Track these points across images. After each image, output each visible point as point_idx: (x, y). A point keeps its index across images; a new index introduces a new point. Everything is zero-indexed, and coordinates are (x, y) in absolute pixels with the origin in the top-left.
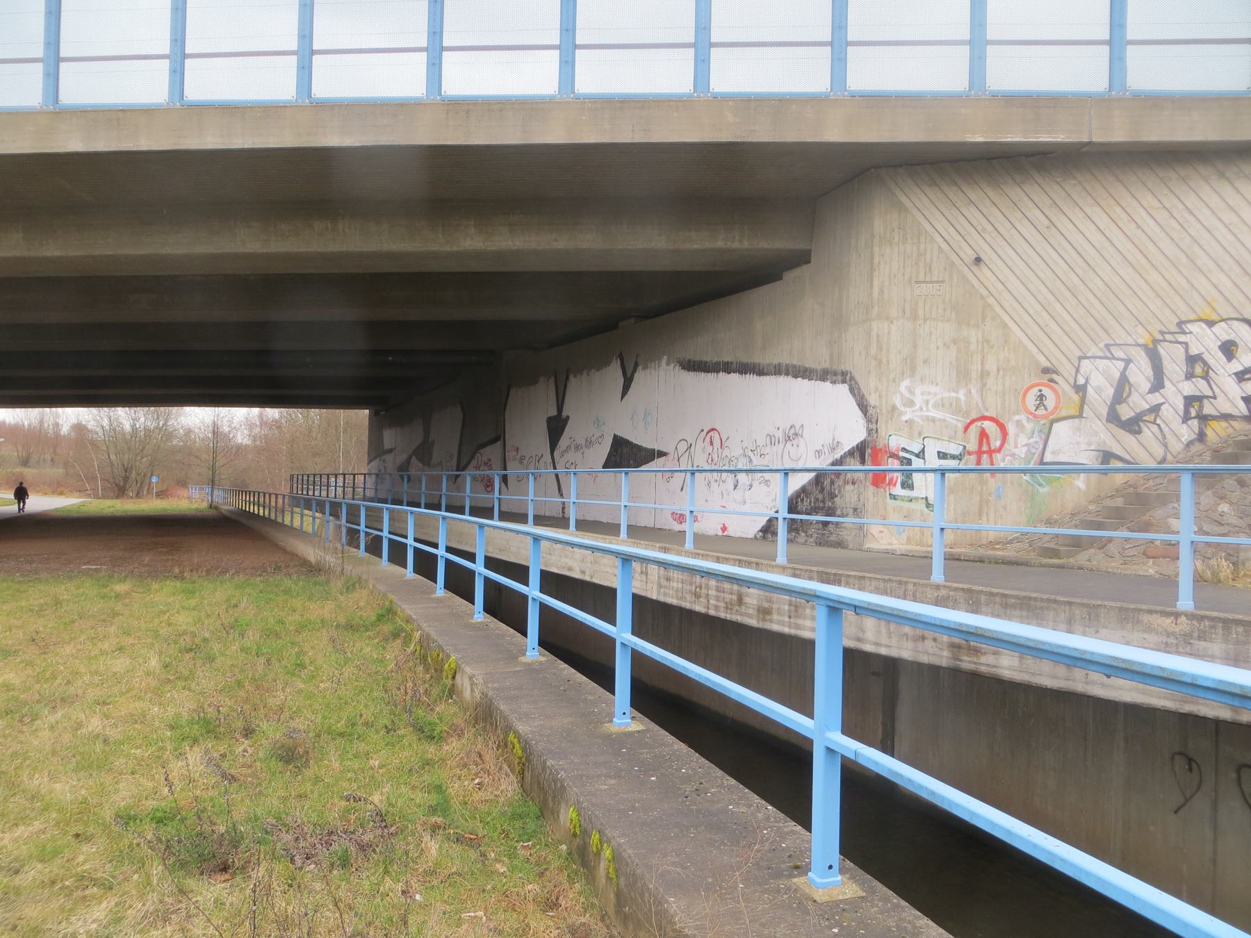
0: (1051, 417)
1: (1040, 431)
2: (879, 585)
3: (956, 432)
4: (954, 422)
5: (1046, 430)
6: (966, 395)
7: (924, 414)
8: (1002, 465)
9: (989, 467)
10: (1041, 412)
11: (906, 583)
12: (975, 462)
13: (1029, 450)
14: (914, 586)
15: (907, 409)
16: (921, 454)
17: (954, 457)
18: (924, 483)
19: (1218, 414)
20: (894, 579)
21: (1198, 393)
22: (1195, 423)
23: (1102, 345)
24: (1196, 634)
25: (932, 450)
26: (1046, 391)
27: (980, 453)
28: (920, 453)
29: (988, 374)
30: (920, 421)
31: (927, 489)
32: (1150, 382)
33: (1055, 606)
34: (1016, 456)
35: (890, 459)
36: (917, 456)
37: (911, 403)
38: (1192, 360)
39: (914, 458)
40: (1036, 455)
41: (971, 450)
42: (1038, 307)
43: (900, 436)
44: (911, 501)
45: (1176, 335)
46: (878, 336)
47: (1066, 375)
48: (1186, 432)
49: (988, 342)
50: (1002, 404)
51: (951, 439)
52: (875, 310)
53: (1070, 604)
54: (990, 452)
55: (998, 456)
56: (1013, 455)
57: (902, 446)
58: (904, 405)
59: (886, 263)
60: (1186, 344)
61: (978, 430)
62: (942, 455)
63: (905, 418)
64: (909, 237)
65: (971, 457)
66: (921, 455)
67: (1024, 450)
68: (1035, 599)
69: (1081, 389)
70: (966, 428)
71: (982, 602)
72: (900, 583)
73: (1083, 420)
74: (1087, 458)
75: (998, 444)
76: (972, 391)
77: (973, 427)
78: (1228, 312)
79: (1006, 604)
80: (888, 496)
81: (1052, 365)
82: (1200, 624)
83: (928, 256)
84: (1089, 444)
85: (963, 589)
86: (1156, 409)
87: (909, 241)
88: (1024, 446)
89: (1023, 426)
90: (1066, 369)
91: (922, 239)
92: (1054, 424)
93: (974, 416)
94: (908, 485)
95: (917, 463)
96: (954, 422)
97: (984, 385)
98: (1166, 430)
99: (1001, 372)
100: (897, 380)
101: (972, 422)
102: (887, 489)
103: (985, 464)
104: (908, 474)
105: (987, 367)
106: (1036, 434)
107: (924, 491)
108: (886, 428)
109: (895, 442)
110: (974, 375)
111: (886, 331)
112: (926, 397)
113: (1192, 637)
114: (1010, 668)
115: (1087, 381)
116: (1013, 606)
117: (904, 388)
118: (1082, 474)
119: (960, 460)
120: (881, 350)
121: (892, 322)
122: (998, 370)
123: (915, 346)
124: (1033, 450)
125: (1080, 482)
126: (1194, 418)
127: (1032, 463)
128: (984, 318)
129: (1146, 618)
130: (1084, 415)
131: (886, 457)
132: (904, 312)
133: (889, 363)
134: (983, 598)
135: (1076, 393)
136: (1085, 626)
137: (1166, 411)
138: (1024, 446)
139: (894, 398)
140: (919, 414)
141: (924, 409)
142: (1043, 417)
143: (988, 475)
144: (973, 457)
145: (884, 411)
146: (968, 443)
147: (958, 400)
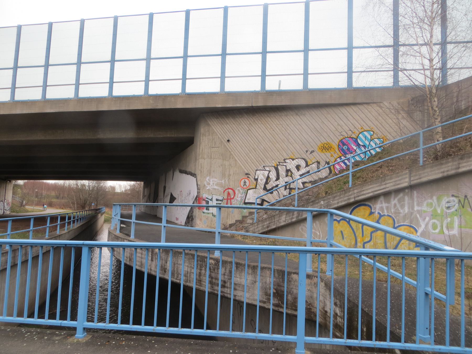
4: (221, 190)
5: (246, 192)
7: (213, 187)
10: (245, 187)
13: (241, 199)
15: (208, 186)
17: (220, 200)
23: (262, 166)
26: (247, 181)
27: (228, 199)
29: (231, 175)
31: (213, 210)
37: (209, 184)
38: (288, 171)
39: (209, 201)
49: (231, 165)
52: (201, 156)
54: (231, 199)
55: (233, 200)
56: (237, 200)
60: (286, 166)
61: (227, 192)
62: (217, 200)
63: (207, 188)
64: (210, 134)
66: (211, 200)
69: (256, 180)
70: (224, 192)
73: (257, 189)
75: (233, 196)
77: (226, 191)
83: (215, 140)
87: (210, 135)
89: (240, 191)
90: (252, 173)
91: (214, 135)
93: (226, 188)
96: (221, 190)
97: (229, 178)
98: (280, 193)
99: (234, 175)
106: (243, 194)
107: (212, 211)
111: (203, 162)
112: (213, 182)
119: (222, 201)
120: (202, 168)
122: (233, 174)
123: (211, 167)
124: (242, 199)
126: (288, 189)
128: (230, 158)
140: (211, 187)
142: (245, 188)
147: (222, 183)
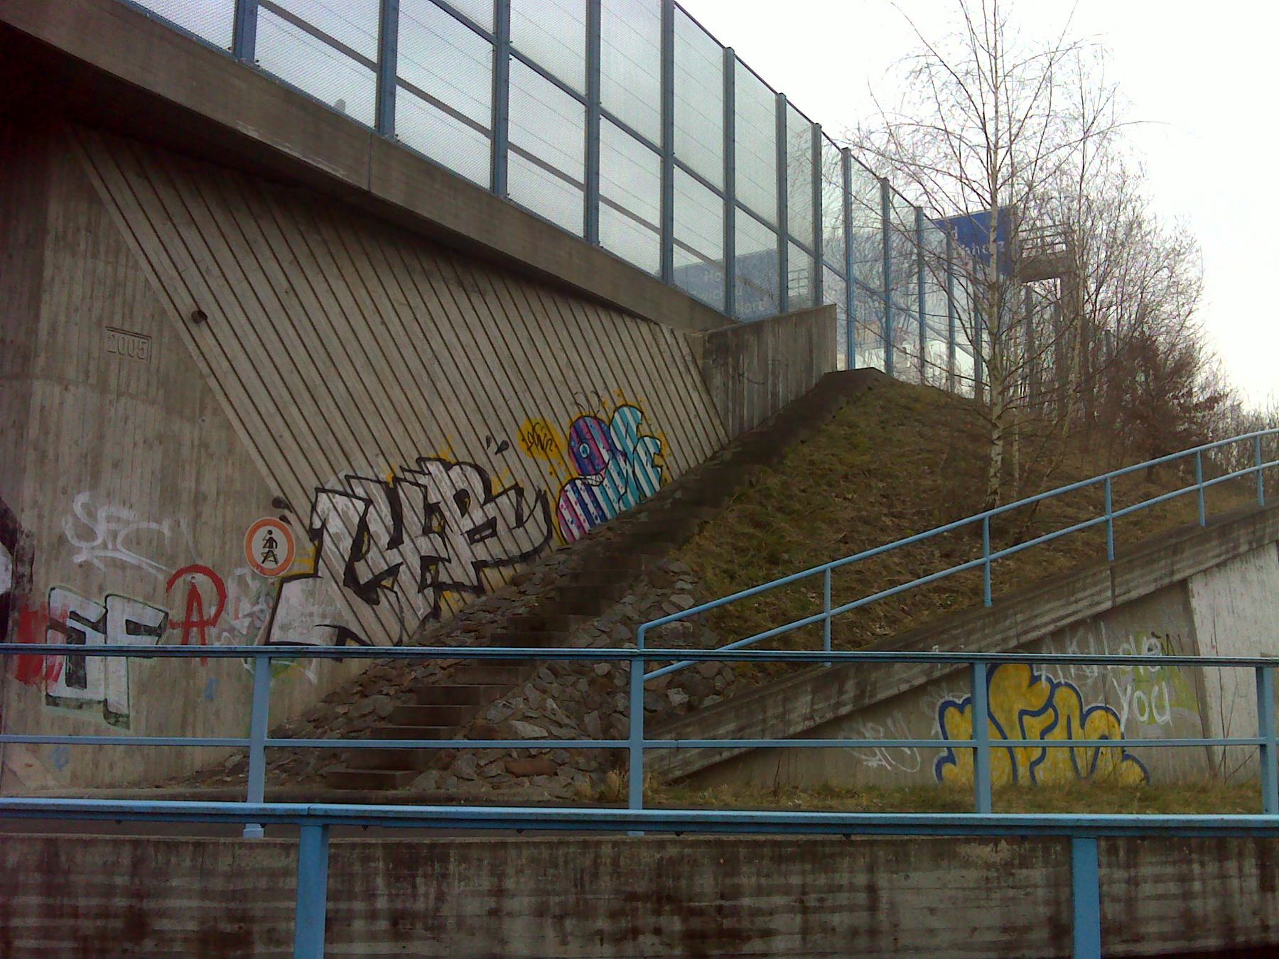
0: (281, 574)
1: (268, 594)
2: (541, 854)
3: (154, 590)
4: (153, 571)
5: (274, 594)
6: (172, 529)
7: (110, 554)
8: (217, 645)
9: (198, 646)
10: (269, 565)
11: (598, 844)
12: (180, 640)
13: (252, 624)
14: (613, 848)
15: (83, 544)
16: (101, 624)
17: (150, 631)
18: (103, 675)
19: (451, 582)
20: (572, 839)
21: (434, 554)
22: (429, 592)
23: (342, 476)
24: (1017, 862)
25: (119, 615)
26: (278, 535)
27: (187, 625)
28: (99, 621)
29: (205, 498)
30: (102, 566)
31: (107, 686)
32: (389, 534)
33: (852, 849)
34: (236, 633)
35: (50, 631)
36: (95, 627)
37: (88, 534)
38: (431, 509)
39: (89, 631)
40: (261, 631)
41: (175, 620)
42: (272, 409)
43: (70, 590)
44: (80, 707)
45: (416, 475)
46: (43, 408)
47: (300, 512)
48: (421, 605)
49: (207, 447)
50: (221, 548)
51: (148, 600)
52: (41, 361)
53: (871, 843)
54: (203, 624)
55: (212, 631)
56: (232, 630)
57: (71, 609)
58: (79, 537)
59: (64, 283)
60: (426, 487)
61: (188, 587)
62: (133, 628)
63: (79, 559)
64: (102, 248)
65: (175, 631)
66: (100, 625)
67: (247, 622)
68: (823, 843)
69: (316, 535)
70: (171, 583)
71: (741, 858)
72: (585, 844)
73: (319, 580)
74: (320, 639)
75: (213, 611)
76: (182, 524)
77: (180, 582)
78: (463, 455)
79: (780, 856)
80: (44, 699)
81: (284, 494)
82: (1020, 848)
83: (129, 289)
84: (324, 616)
85: (708, 842)
86: (393, 571)
87: (102, 256)
88: (245, 616)
89: (247, 585)
90: (302, 505)
91: (123, 260)
92: (285, 585)
93: (182, 564)
94: (77, 679)
95: (94, 639)
96: (153, 571)
97: (199, 515)
98: (403, 600)
99: (222, 498)
100: (70, 489)
101: (179, 573)
102: (43, 687)
103: (194, 645)
104: (78, 657)
105: (203, 488)
106: (262, 599)
107: (102, 689)
108: (47, 573)
109: (62, 600)
110: (185, 498)
111: (57, 401)
112: (113, 526)
113: (1013, 865)
114: (1163, 937)
115: (324, 525)
116: (790, 859)
117: (79, 504)
118: (314, 660)
119: (160, 636)
120: (47, 433)
121: (66, 388)
122: (218, 494)
123: (101, 437)
124: (258, 624)
125: (311, 671)
126: (430, 586)
127: (256, 642)
128: (203, 408)
129: (963, 850)
130: (320, 574)
131: (44, 628)
132: (87, 373)
133: (57, 460)
134: (743, 851)
135: (311, 540)
136: (892, 873)
137: (403, 573)
138: (245, 616)
139: (63, 522)
140: (102, 553)
141: (110, 546)
142: (273, 573)
143: (197, 661)
144: (178, 632)
145: (45, 543)
146: (171, 609)
147: (160, 533)
